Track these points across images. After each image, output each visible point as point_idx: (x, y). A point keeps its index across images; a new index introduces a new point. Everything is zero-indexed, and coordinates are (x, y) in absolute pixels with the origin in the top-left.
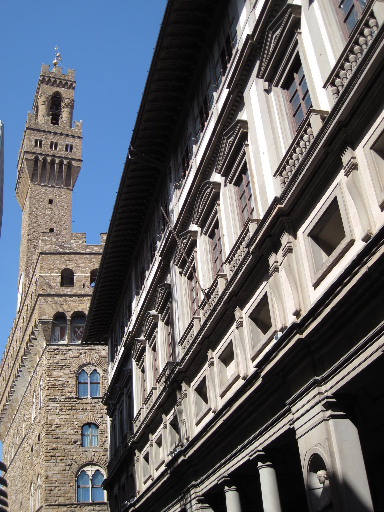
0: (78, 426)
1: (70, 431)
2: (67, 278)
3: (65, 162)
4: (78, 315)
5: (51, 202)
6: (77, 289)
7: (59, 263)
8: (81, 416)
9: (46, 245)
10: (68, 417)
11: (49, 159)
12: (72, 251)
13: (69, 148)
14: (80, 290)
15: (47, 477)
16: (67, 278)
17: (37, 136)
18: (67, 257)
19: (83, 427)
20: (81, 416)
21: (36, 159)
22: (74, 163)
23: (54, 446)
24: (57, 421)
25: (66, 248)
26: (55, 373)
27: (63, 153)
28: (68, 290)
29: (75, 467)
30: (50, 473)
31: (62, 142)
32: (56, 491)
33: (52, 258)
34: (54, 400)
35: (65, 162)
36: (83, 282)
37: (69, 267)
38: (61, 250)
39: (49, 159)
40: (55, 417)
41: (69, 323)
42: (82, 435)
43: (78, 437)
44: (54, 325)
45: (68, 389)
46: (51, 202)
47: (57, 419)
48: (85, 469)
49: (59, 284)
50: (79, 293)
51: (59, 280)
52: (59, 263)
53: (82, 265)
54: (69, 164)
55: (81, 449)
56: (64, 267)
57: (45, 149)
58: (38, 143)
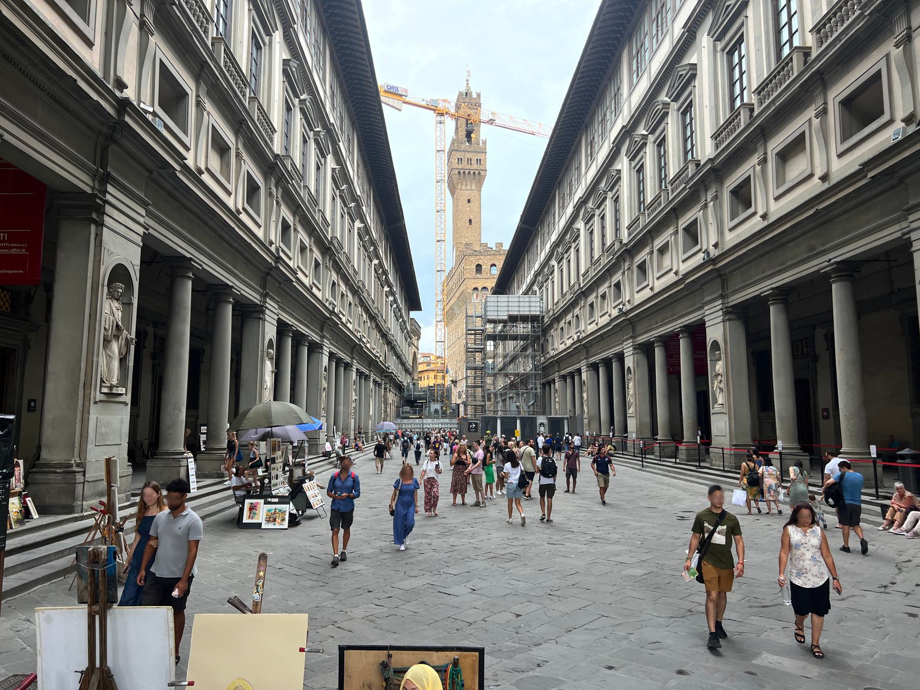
2: (479, 268)
3: (477, 172)
4: (485, 288)
5: (469, 201)
6: (484, 275)
11: (467, 172)
13: (479, 161)
16: (479, 268)
17: (459, 155)
21: (459, 172)
22: (482, 173)
27: (475, 166)
31: (474, 157)
35: (477, 172)
39: (467, 172)
46: (469, 201)
52: (474, 261)
54: (479, 173)
57: (465, 165)
58: (460, 160)
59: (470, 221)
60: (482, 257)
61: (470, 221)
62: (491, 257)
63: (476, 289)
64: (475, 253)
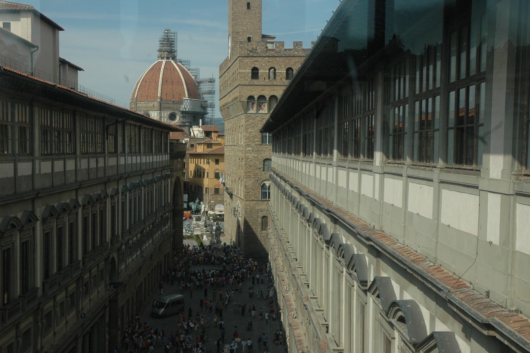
0: (261, 159)
1: (257, 163)
4: (262, 97)
6: (260, 81)
7: (250, 63)
8: (263, 155)
9: (242, 51)
10: (256, 155)
12: (258, 55)
14: (262, 81)
15: (246, 186)
18: (254, 59)
19: (264, 161)
20: (263, 155)
23: (249, 170)
24: (251, 157)
25: (254, 52)
26: (249, 130)
28: (255, 82)
29: (260, 181)
30: (247, 184)
32: (250, 193)
33: (246, 60)
34: (249, 146)
36: (264, 76)
37: (256, 66)
38: (251, 54)
40: (250, 155)
41: (256, 102)
42: (264, 165)
43: (262, 166)
44: (248, 102)
45: (257, 140)
47: (251, 156)
48: (265, 182)
49: (250, 78)
50: (262, 83)
51: (250, 75)
52: (250, 63)
53: (264, 65)
55: (263, 173)
56: (253, 66)
59: (249, 4)
60: (260, 59)
61: (249, 4)
62: (270, 59)
63: (251, 98)
64: (252, 54)
